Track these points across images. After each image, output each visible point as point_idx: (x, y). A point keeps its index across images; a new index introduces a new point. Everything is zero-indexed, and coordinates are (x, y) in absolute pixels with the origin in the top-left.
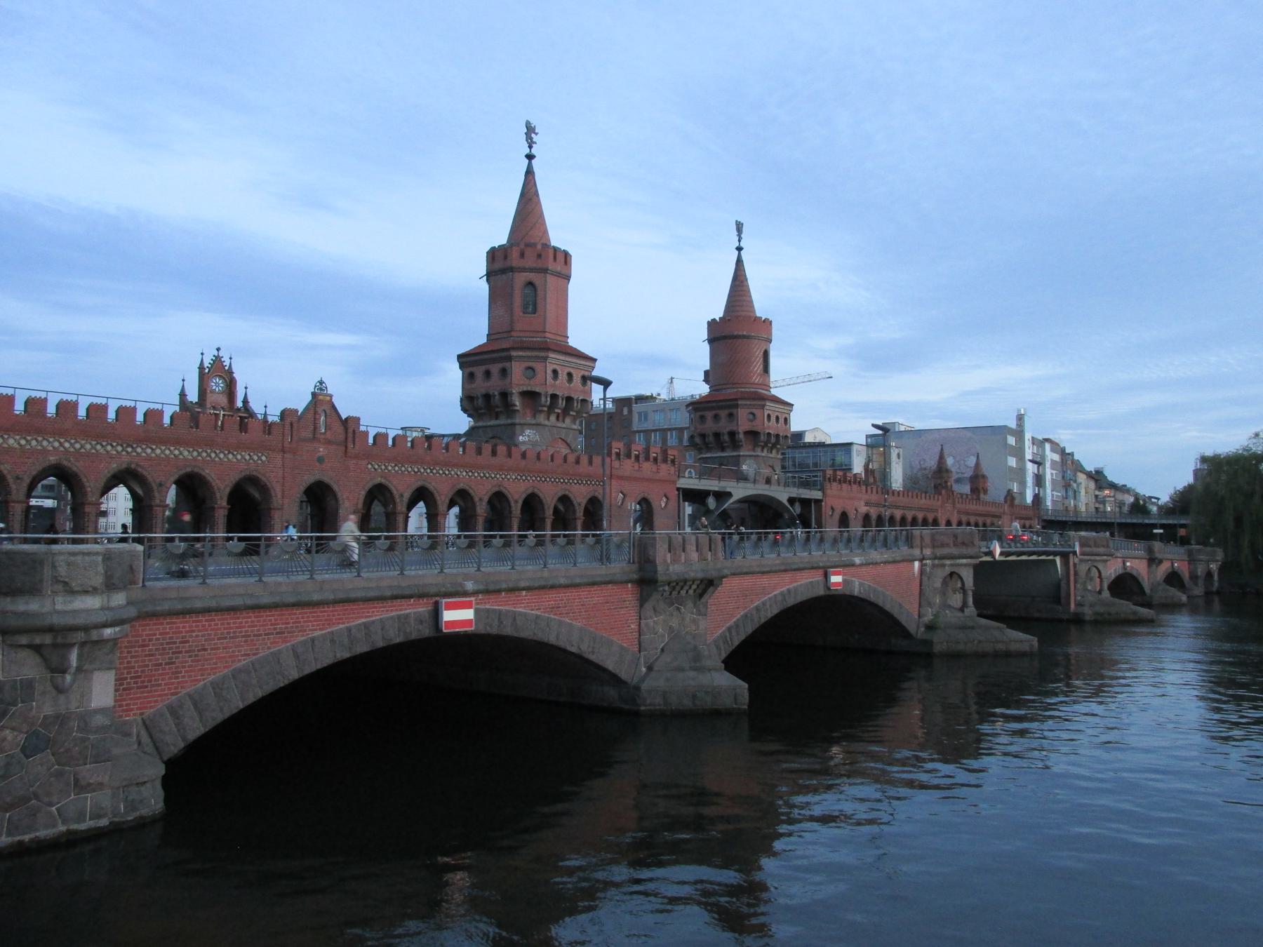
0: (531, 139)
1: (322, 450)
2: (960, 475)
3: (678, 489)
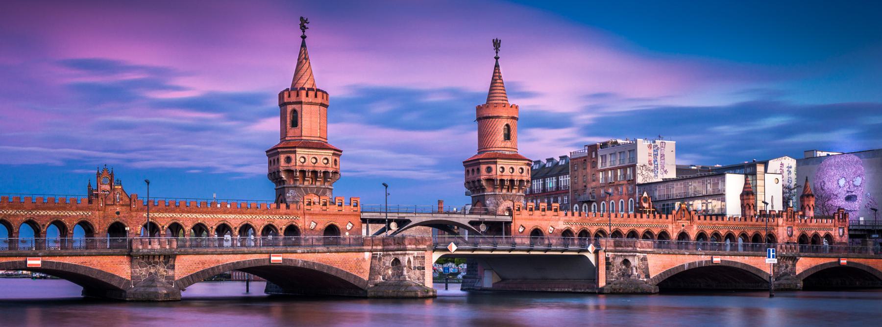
1: (118, 209)
2: (850, 194)
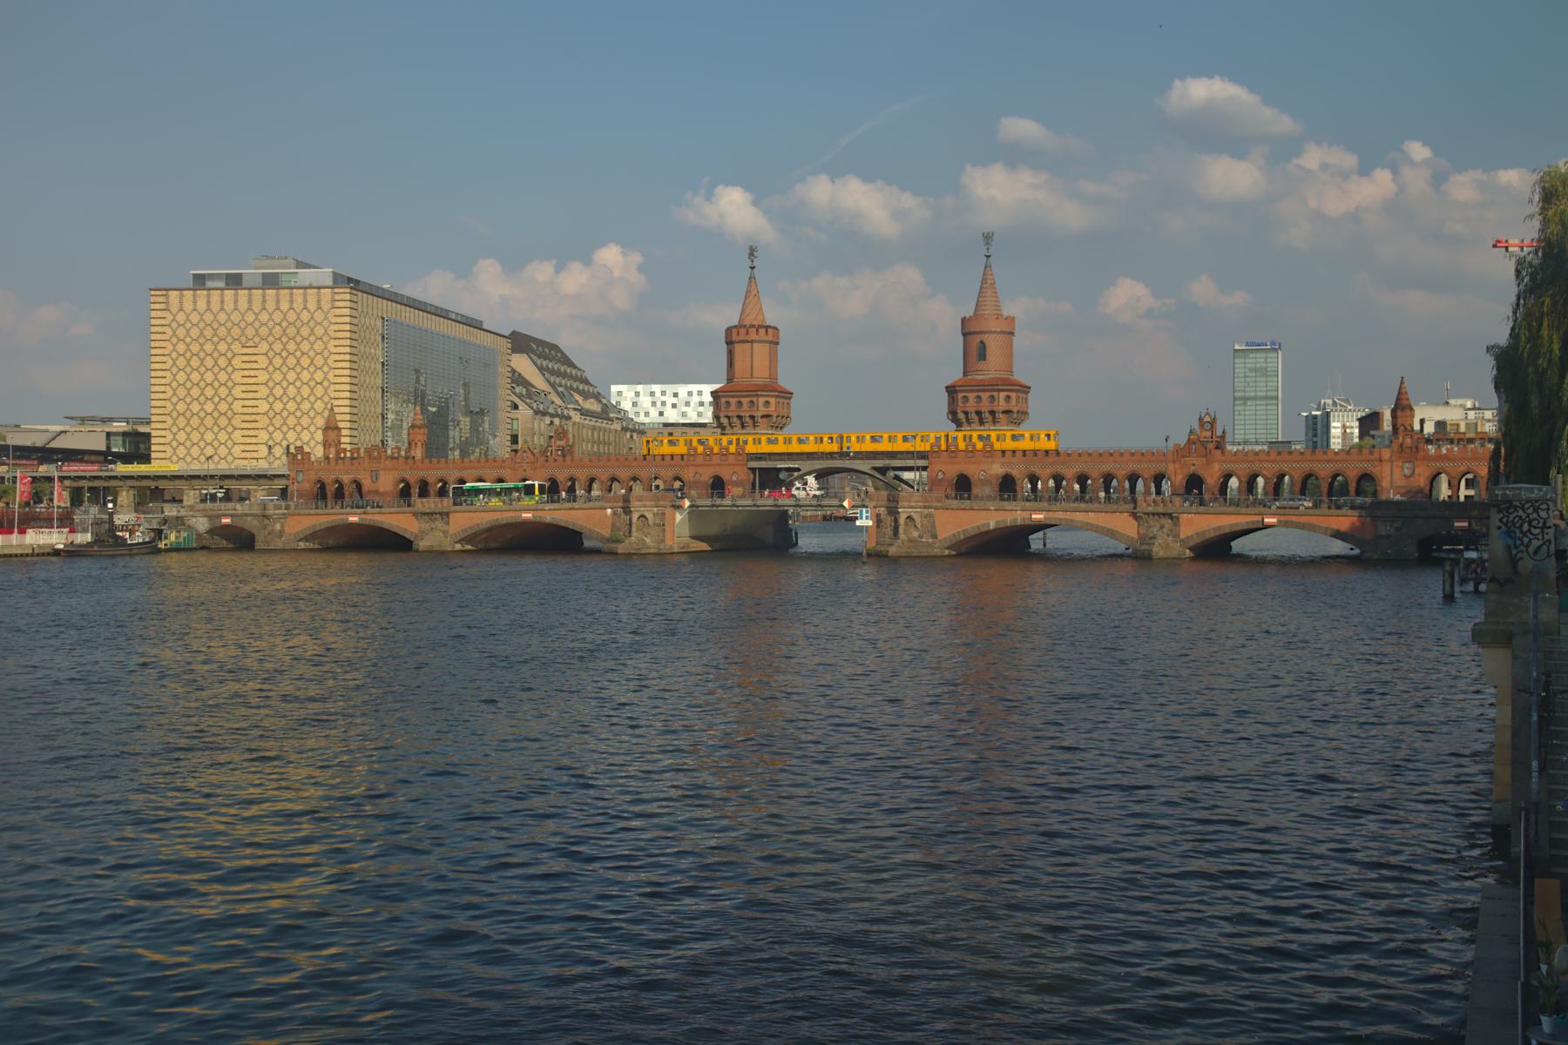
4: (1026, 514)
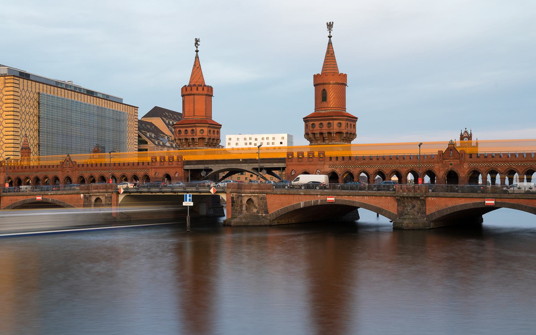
0: (197, 44)
3: (185, 170)
4: (323, 198)
